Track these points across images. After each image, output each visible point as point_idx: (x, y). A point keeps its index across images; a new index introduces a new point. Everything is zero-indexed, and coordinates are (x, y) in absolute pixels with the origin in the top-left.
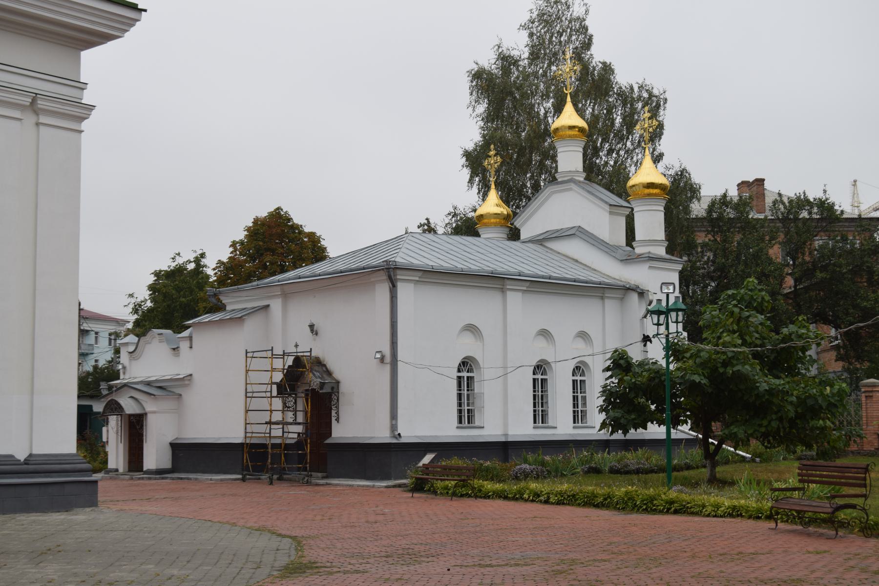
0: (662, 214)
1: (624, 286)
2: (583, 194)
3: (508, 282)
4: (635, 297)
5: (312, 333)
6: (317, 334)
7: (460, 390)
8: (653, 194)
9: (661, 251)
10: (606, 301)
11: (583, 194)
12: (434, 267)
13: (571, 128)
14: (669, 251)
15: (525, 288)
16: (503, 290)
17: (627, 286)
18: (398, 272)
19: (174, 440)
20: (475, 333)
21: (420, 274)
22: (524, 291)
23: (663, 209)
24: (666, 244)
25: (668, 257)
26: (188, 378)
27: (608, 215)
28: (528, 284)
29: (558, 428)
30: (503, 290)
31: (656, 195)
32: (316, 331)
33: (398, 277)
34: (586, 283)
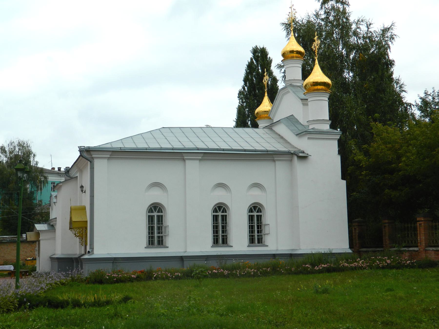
0: (327, 103)
1: (289, 152)
2: (316, 94)
3: (184, 155)
4: (295, 158)
5: (82, 191)
6: (85, 192)
7: (151, 224)
8: (320, 89)
9: (326, 127)
10: (187, 162)
11: (316, 94)
12: (122, 149)
13: (292, 52)
14: (333, 126)
15: (200, 158)
16: (184, 160)
17: (292, 152)
18: (92, 153)
19: (50, 256)
20: (225, 187)
21: (110, 153)
22: (200, 160)
23: (327, 100)
24: (330, 122)
25: (331, 130)
26: (55, 220)
27: (302, 105)
28: (202, 155)
29: (269, 246)
30: (184, 160)
31: (322, 89)
32: (85, 190)
33: (93, 156)
34: (255, 152)
